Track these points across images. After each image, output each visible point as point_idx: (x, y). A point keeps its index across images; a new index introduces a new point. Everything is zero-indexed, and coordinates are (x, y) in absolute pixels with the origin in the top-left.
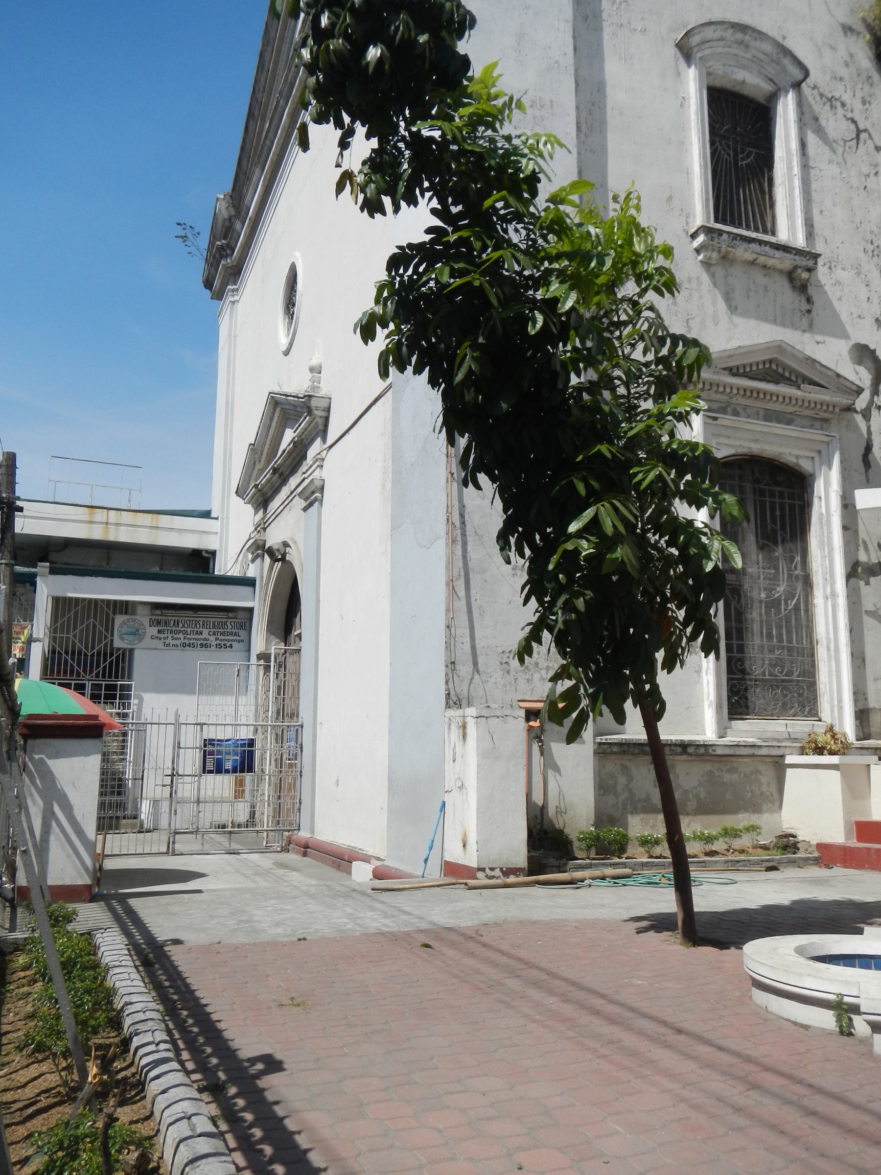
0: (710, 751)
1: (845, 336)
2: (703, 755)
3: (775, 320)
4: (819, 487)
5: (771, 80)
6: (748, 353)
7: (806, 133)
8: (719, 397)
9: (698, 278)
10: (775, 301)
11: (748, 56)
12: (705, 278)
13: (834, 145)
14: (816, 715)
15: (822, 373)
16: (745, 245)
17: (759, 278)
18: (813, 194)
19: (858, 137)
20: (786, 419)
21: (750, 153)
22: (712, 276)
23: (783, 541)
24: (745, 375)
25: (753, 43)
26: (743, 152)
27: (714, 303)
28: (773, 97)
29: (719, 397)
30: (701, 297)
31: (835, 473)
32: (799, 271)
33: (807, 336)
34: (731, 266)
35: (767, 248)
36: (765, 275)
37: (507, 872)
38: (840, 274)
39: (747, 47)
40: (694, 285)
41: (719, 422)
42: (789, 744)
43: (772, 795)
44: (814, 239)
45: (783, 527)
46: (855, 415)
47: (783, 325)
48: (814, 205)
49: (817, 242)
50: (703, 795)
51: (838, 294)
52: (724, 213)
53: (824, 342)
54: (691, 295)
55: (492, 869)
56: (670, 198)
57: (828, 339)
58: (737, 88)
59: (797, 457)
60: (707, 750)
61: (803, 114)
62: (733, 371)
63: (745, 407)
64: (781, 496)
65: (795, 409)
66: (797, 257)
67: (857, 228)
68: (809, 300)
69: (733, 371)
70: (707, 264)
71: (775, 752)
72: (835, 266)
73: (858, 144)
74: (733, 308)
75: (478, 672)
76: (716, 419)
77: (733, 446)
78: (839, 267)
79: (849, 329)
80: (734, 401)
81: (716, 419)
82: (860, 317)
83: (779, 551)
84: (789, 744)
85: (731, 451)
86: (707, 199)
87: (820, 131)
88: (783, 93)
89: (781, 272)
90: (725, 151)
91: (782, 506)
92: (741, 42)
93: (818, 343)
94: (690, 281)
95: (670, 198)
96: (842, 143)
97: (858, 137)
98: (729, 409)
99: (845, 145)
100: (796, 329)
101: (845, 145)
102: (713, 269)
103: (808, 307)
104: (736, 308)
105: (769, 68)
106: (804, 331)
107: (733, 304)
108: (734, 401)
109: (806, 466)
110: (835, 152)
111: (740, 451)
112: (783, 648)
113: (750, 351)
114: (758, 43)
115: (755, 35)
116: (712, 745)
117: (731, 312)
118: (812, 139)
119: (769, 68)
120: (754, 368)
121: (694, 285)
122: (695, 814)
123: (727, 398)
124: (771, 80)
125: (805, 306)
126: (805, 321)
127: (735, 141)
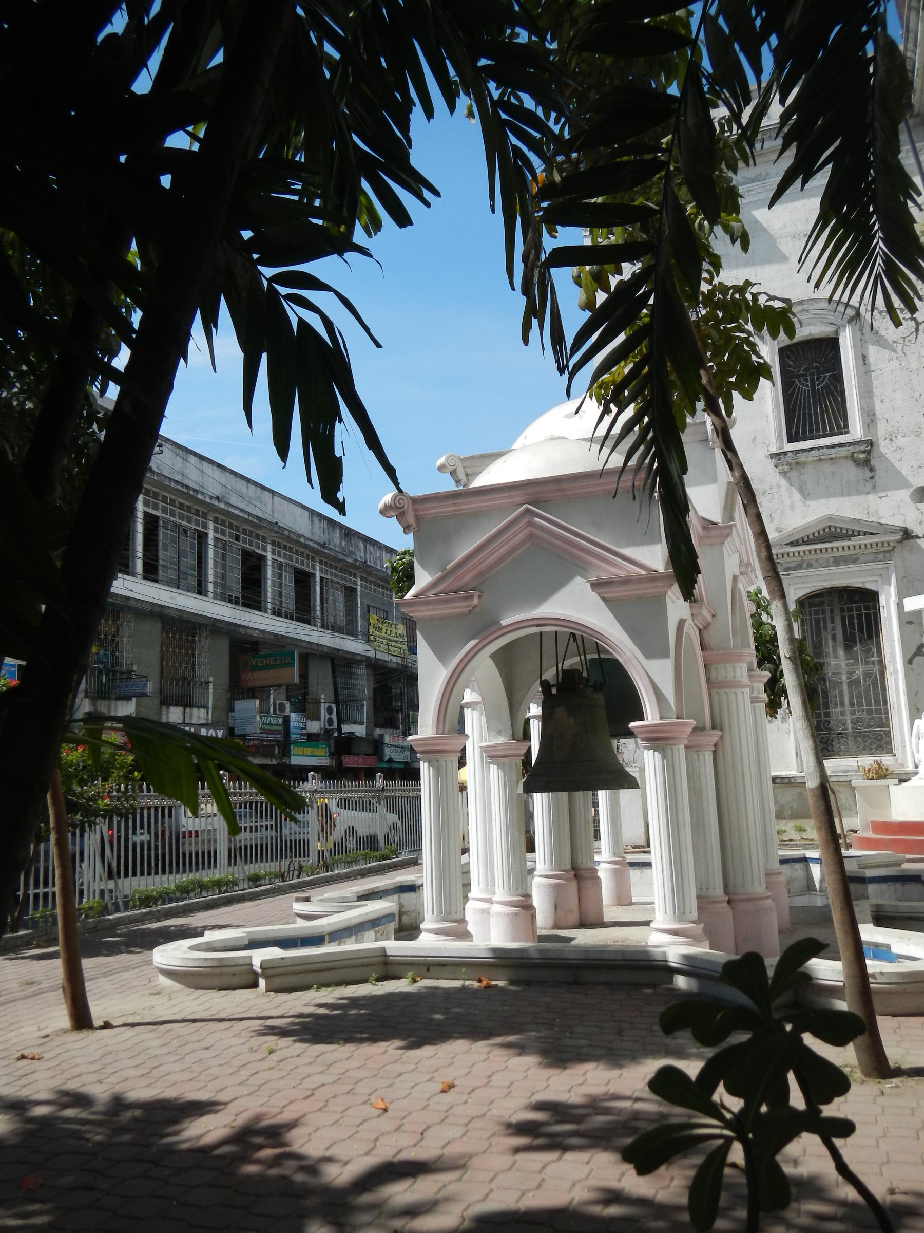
0: (793, 781)
1: (907, 485)
2: (787, 783)
3: (842, 492)
4: (882, 599)
5: (832, 324)
6: (803, 529)
7: (867, 348)
8: (792, 559)
9: (777, 484)
10: (841, 480)
11: (811, 316)
12: (783, 482)
13: (894, 345)
14: (892, 753)
15: (868, 525)
16: (806, 454)
17: (828, 468)
18: (875, 390)
19: (917, 330)
20: (854, 560)
21: (825, 377)
22: (789, 480)
23: (861, 641)
24: (804, 543)
25: (811, 308)
26: (818, 378)
27: (791, 497)
28: (837, 333)
29: (792, 559)
30: (781, 496)
31: (893, 589)
32: (855, 455)
33: (871, 497)
34: (804, 467)
35: (825, 450)
36: (832, 464)
37: (635, 847)
38: (901, 441)
39: (807, 311)
40: (775, 490)
41: (791, 576)
42: (854, 773)
43: (850, 805)
44: (876, 423)
45: (861, 630)
46: (918, 540)
47: (850, 494)
48: (875, 398)
49: (878, 425)
50: (795, 806)
51: (899, 457)
52: (797, 433)
53: (887, 496)
54: (772, 498)
55: (627, 846)
56: (755, 438)
57: (889, 493)
58: (810, 337)
59: (863, 583)
60: (790, 781)
61: (863, 334)
62: (792, 544)
63: (817, 561)
64: (859, 609)
65: (856, 552)
66: (850, 448)
67: (917, 400)
68: (872, 470)
69: (792, 544)
70: (784, 473)
71: (848, 779)
72: (896, 437)
73: (917, 334)
74: (805, 494)
75: (638, 748)
76: (789, 575)
77: (808, 587)
78: (899, 437)
79: (910, 479)
80: (805, 558)
81: (789, 575)
82: (920, 467)
83: (858, 648)
84: (854, 773)
85: (809, 591)
86: (780, 431)
87: (880, 341)
88: (842, 329)
89: (846, 457)
90: (803, 384)
91: (860, 617)
92: (803, 310)
93: (880, 498)
94: (771, 487)
95: (755, 438)
96: (902, 341)
97: (917, 330)
98: (805, 565)
99: (904, 341)
100: (861, 494)
101: (904, 341)
102: (788, 474)
103: (871, 475)
104: (809, 494)
105: (828, 317)
106: (868, 493)
107: (806, 493)
108: (805, 558)
109: (870, 586)
110: (895, 351)
111: (814, 589)
112: (863, 710)
113: (805, 527)
114: (816, 306)
115: (810, 302)
116: (793, 777)
117: (805, 498)
118: (873, 352)
119: (828, 317)
120: (822, 532)
121: (775, 490)
122: (790, 819)
123: (799, 559)
124: (832, 324)
125: (868, 474)
126: (869, 486)
127: (812, 374)
